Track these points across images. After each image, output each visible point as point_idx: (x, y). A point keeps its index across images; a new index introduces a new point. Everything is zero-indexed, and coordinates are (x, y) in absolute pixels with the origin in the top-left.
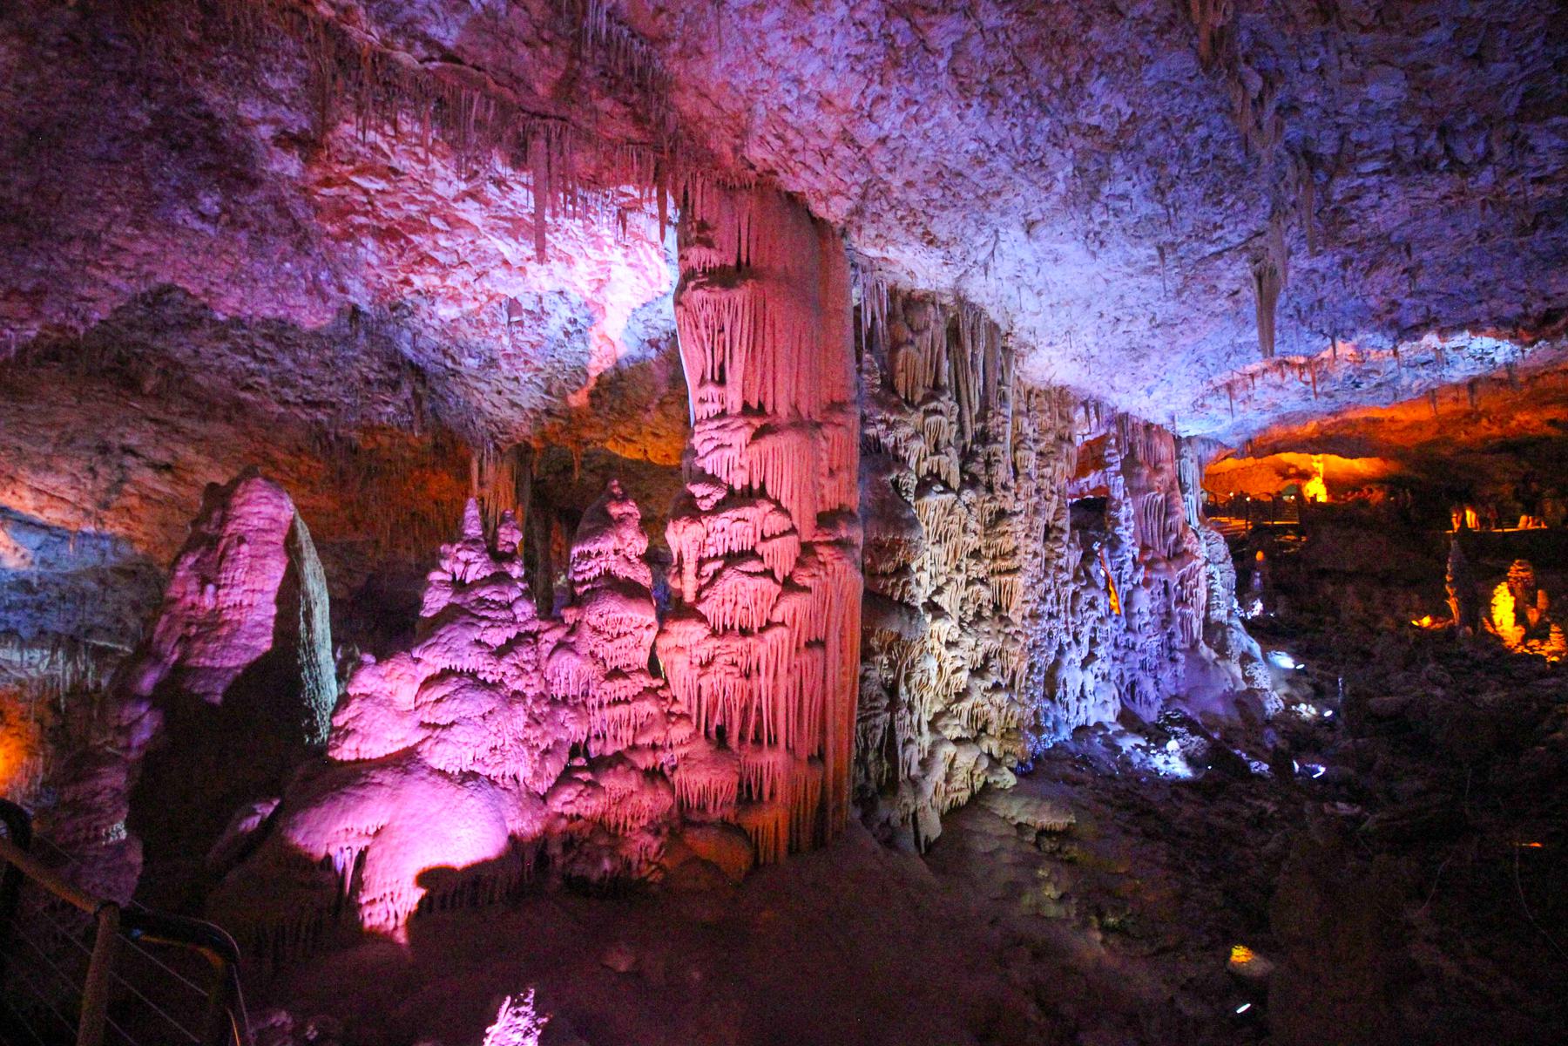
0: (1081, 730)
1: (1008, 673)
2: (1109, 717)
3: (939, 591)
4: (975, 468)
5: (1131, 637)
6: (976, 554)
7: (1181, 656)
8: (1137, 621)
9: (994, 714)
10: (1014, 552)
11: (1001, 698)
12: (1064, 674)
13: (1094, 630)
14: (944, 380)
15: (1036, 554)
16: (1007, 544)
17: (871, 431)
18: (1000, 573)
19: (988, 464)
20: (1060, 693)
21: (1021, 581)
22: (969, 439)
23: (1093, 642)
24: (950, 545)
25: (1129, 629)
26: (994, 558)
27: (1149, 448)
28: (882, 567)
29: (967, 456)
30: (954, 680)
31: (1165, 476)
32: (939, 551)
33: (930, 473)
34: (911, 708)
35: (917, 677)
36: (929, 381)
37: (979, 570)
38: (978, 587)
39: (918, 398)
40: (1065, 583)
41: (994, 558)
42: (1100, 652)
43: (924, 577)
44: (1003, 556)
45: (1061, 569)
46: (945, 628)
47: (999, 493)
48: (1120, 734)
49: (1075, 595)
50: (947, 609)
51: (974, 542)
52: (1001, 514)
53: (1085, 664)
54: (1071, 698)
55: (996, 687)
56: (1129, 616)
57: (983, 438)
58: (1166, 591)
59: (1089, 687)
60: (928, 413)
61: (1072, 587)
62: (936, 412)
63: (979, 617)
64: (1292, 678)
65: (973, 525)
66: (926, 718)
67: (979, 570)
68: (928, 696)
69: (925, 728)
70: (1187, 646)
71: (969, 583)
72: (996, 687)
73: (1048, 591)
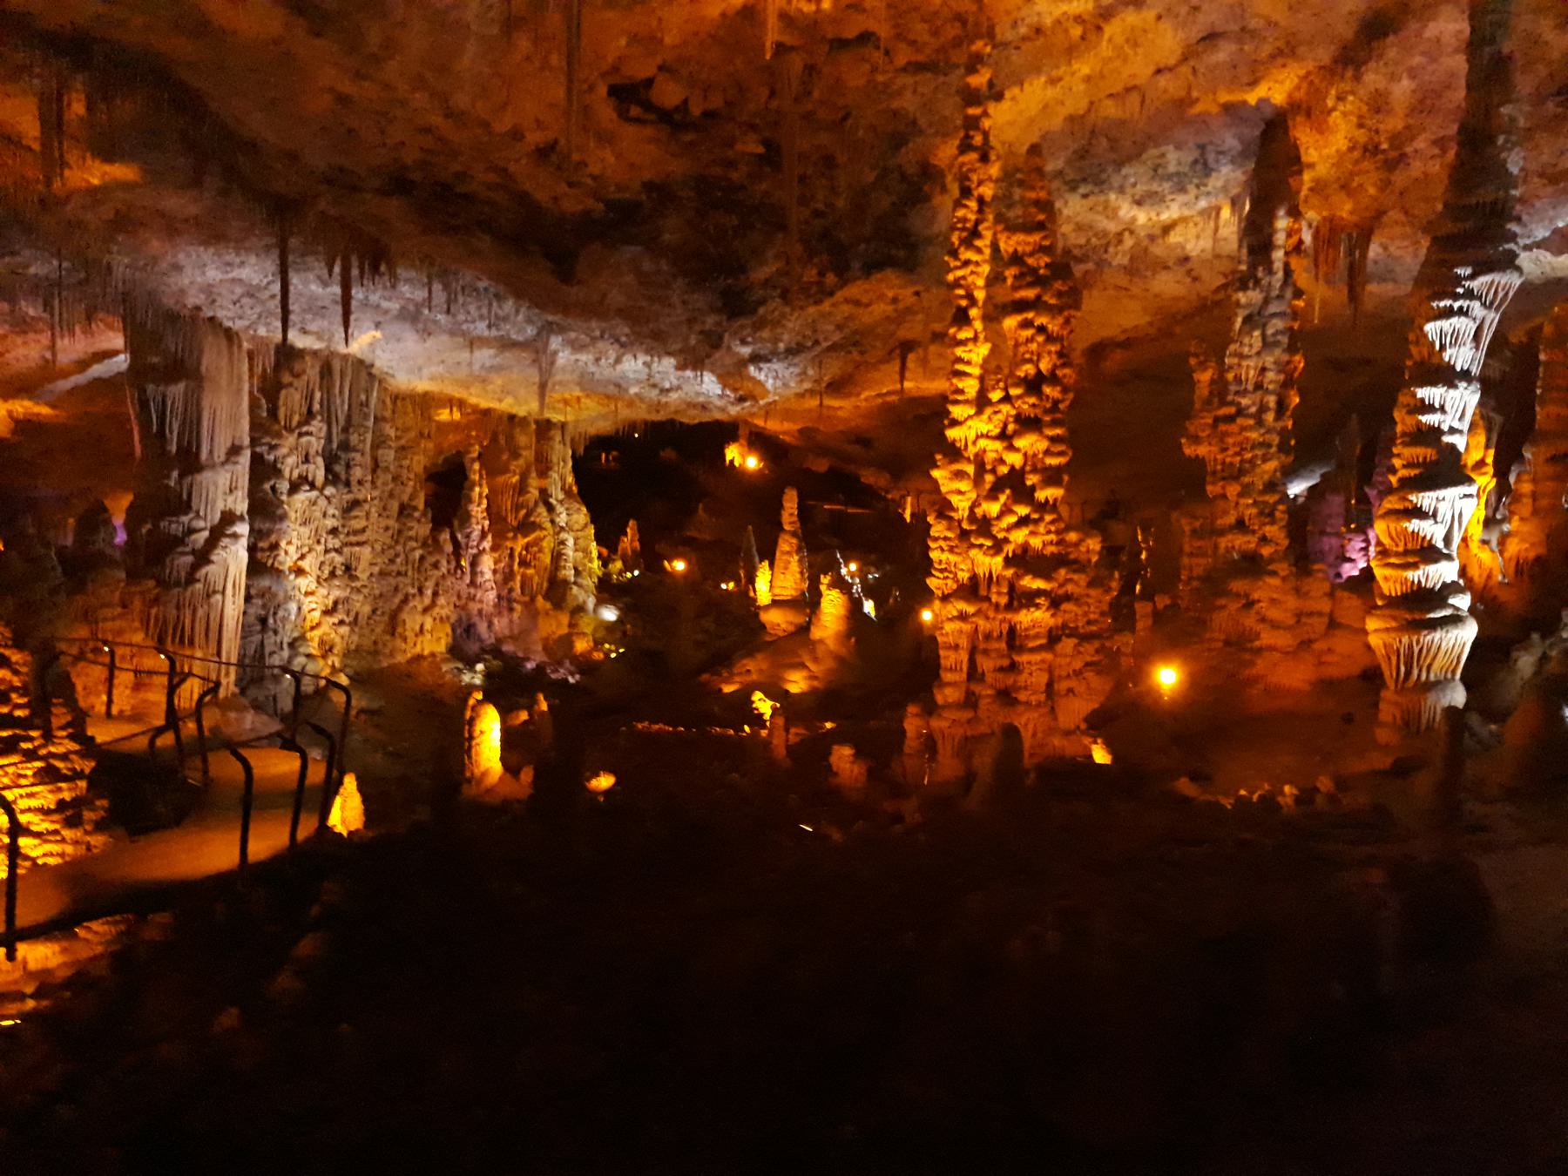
0: (419, 658)
1: (353, 614)
2: (441, 648)
3: (302, 557)
4: (339, 468)
5: (472, 591)
6: (334, 532)
7: (518, 607)
8: (479, 580)
9: (338, 640)
10: (363, 530)
11: (344, 630)
12: (404, 616)
13: (437, 585)
14: (316, 407)
15: (387, 529)
16: (357, 524)
17: (258, 449)
18: (352, 544)
19: (348, 466)
20: (400, 630)
21: (366, 552)
22: (335, 446)
23: (435, 594)
24: (313, 526)
25: (473, 583)
26: (348, 534)
27: (510, 438)
28: (261, 545)
29: (330, 460)
30: (309, 617)
31: (521, 462)
32: (305, 531)
33: (300, 477)
34: (276, 632)
35: (281, 613)
36: (304, 410)
37: (336, 543)
38: (333, 554)
39: (294, 423)
40: (414, 549)
41: (348, 534)
42: (442, 600)
43: (292, 549)
44: (356, 533)
45: (411, 538)
46: (305, 583)
47: (355, 488)
48: (445, 660)
49: (422, 558)
50: (307, 569)
51: (330, 523)
52: (356, 504)
53: (426, 610)
54: (409, 634)
55: (341, 622)
56: (474, 573)
57: (345, 446)
58: (511, 556)
59: (428, 626)
60: (301, 435)
61: (418, 554)
62: (309, 434)
63: (333, 574)
64: (610, 627)
65: (331, 511)
66: (286, 640)
67: (334, 542)
68: (289, 627)
69: (285, 646)
70: (527, 599)
71: (327, 551)
72: (341, 622)
73: (397, 555)
